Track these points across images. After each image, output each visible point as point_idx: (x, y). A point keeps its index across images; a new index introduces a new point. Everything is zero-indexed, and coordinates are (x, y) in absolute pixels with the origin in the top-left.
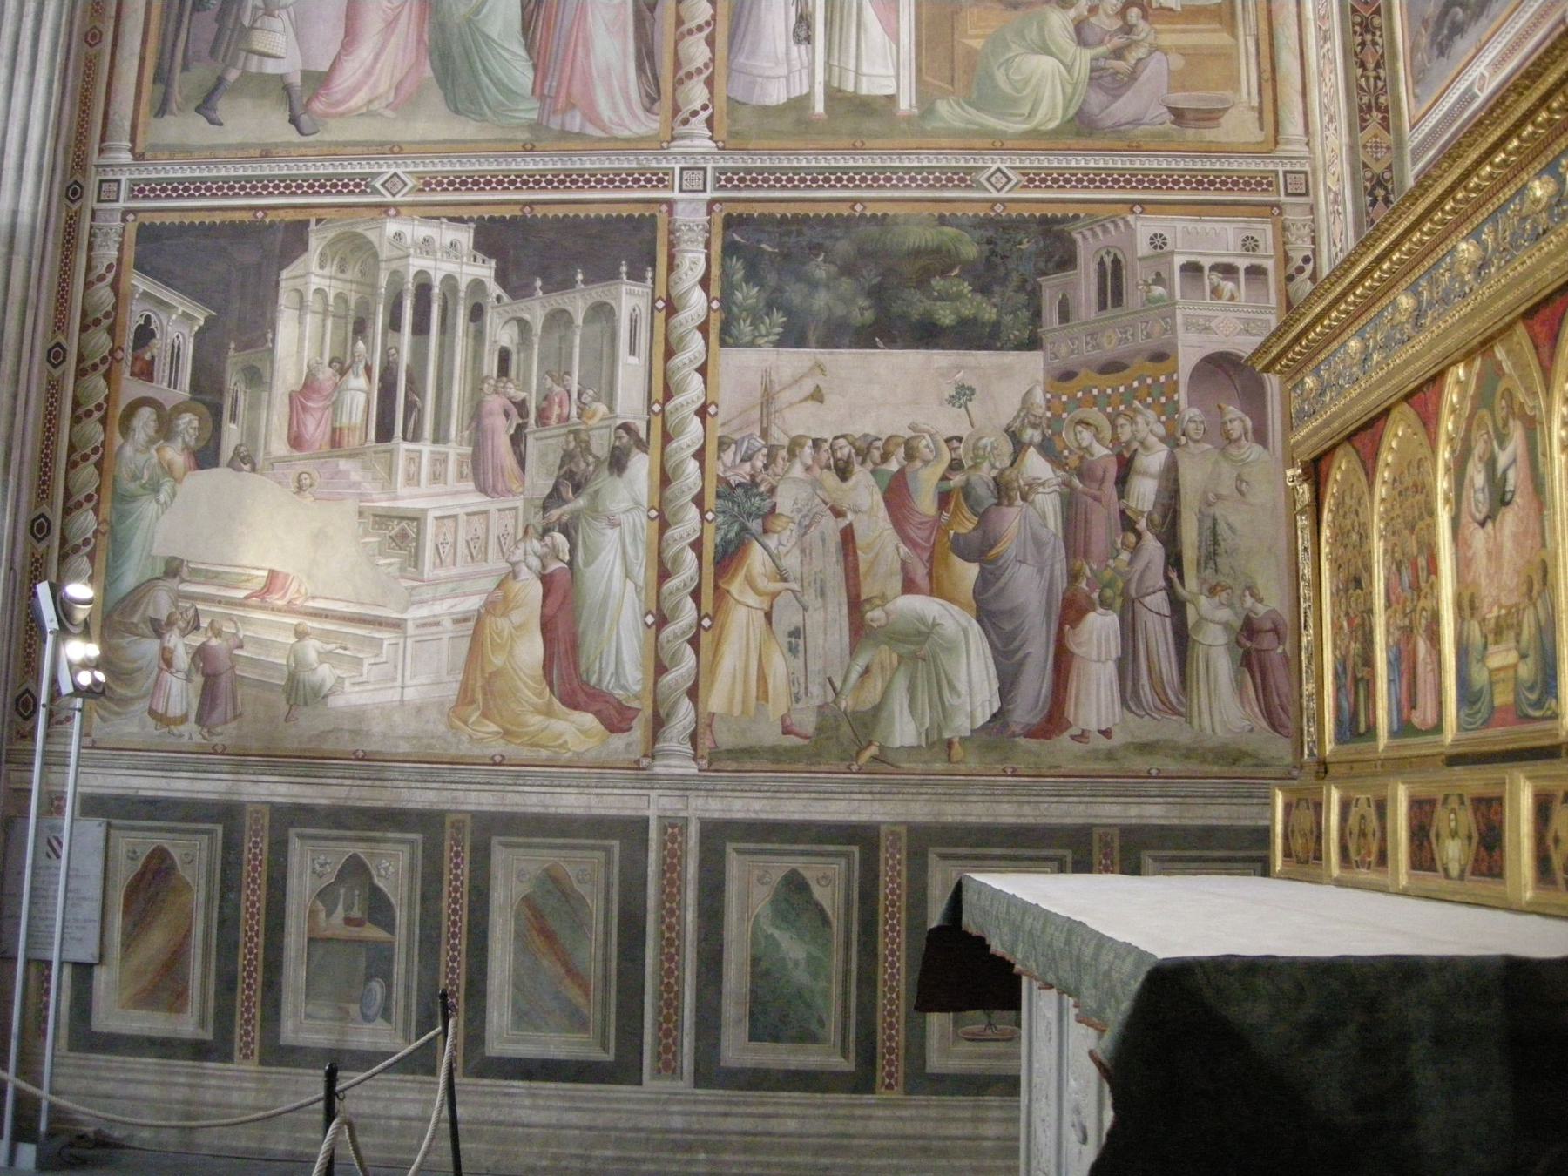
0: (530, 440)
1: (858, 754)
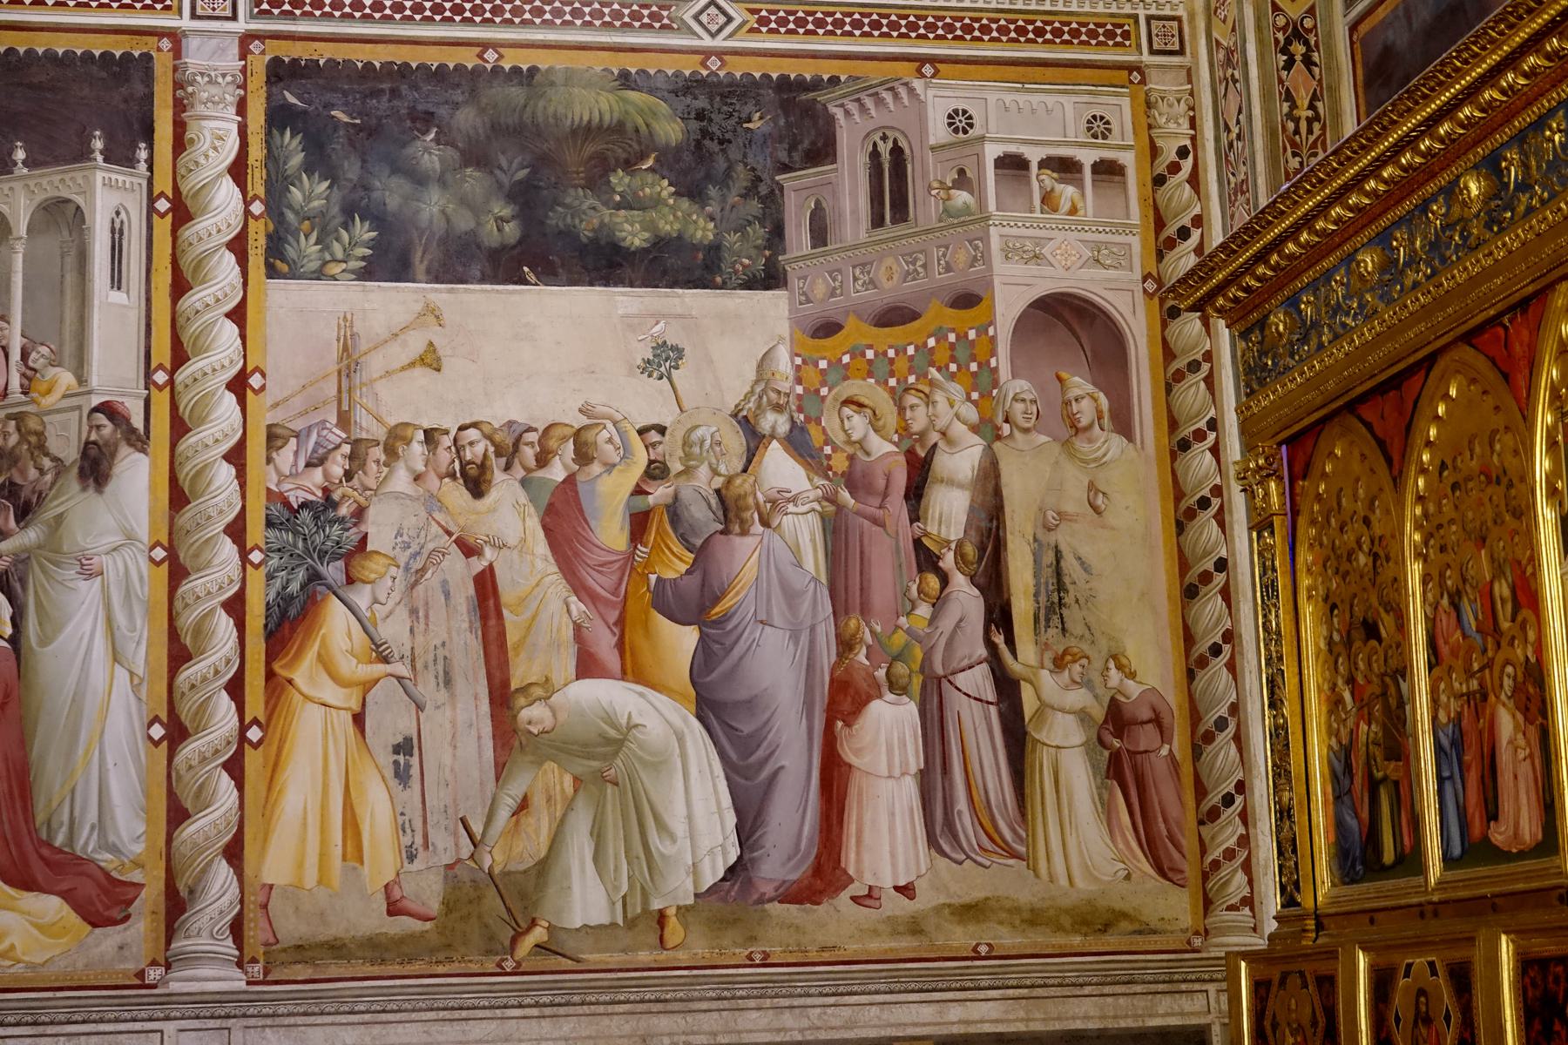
1: (514, 941)
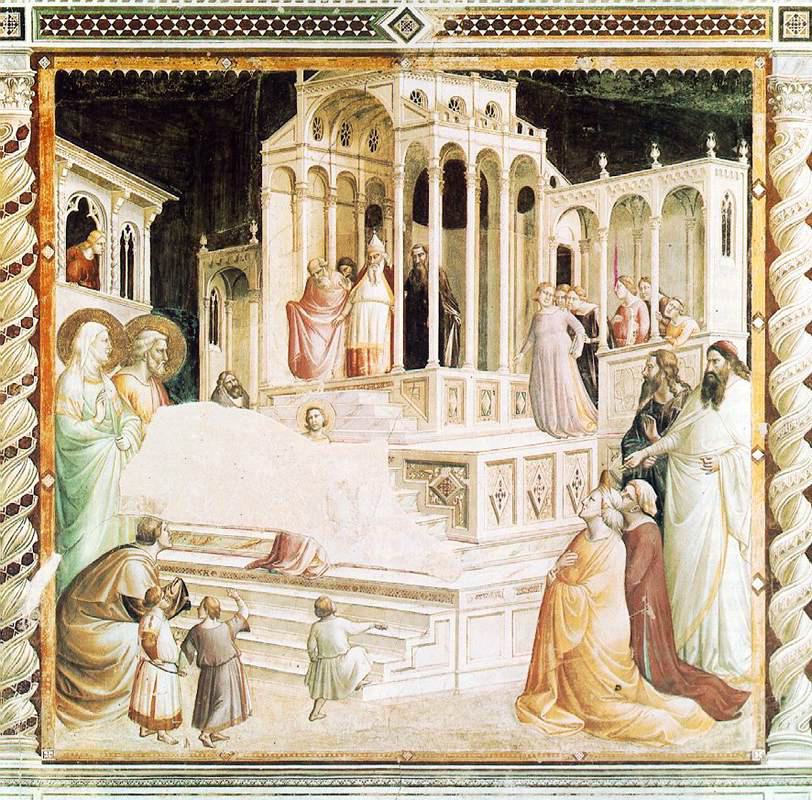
0: (602, 363)
